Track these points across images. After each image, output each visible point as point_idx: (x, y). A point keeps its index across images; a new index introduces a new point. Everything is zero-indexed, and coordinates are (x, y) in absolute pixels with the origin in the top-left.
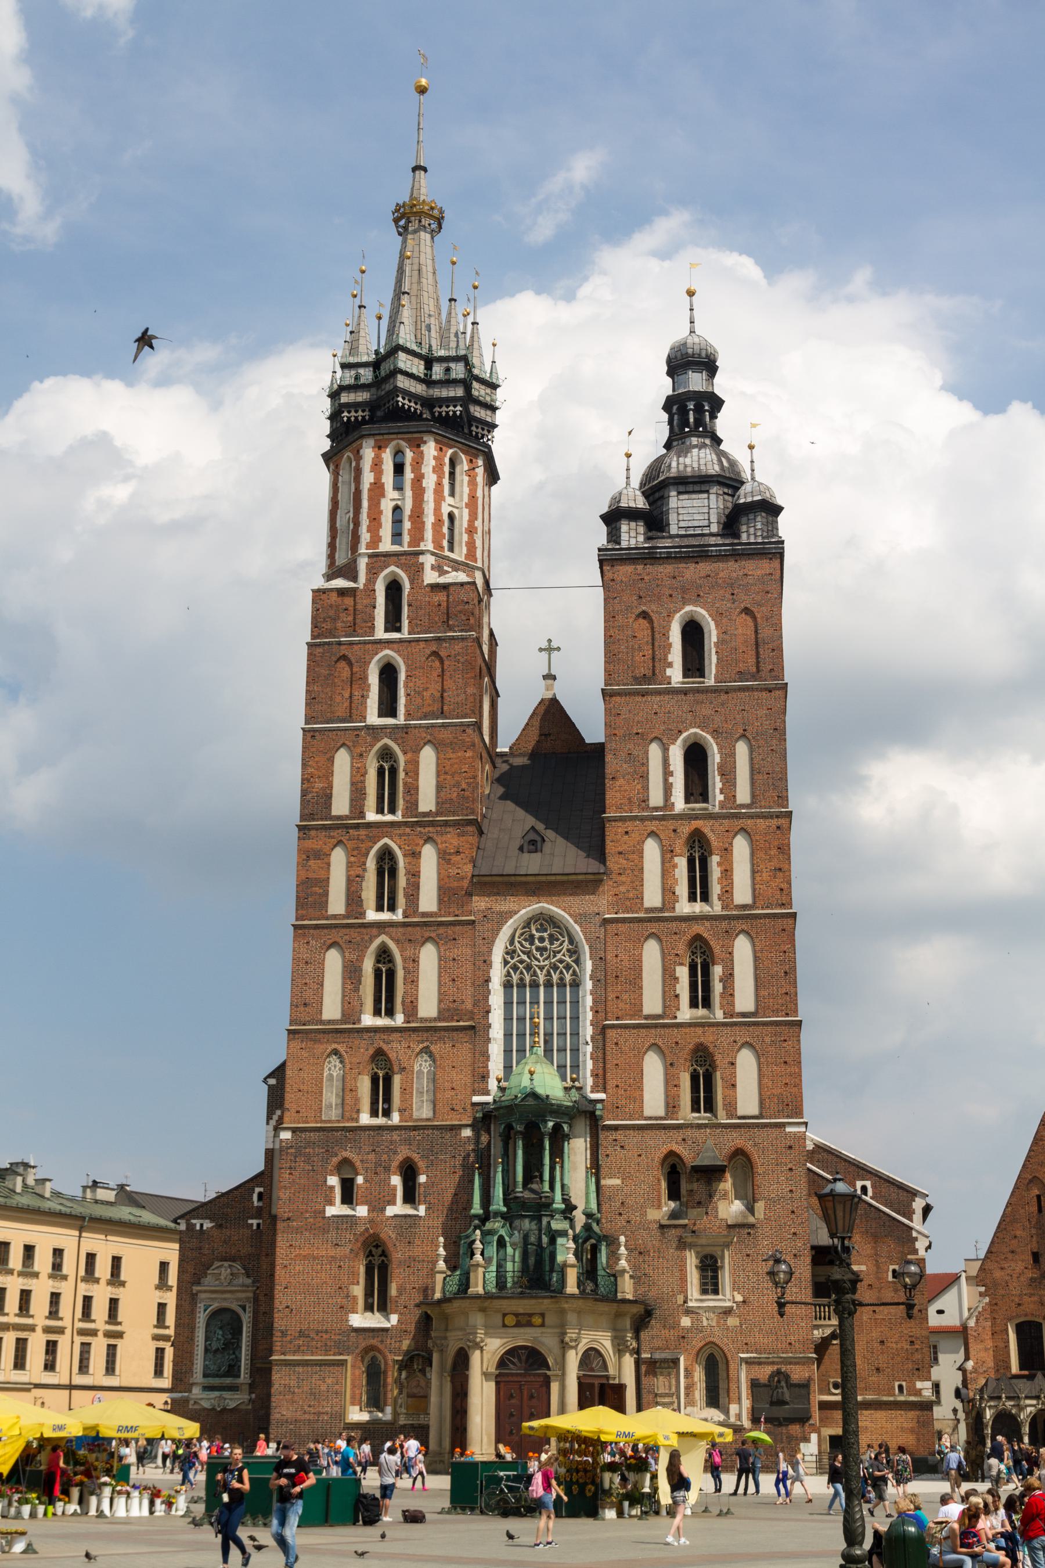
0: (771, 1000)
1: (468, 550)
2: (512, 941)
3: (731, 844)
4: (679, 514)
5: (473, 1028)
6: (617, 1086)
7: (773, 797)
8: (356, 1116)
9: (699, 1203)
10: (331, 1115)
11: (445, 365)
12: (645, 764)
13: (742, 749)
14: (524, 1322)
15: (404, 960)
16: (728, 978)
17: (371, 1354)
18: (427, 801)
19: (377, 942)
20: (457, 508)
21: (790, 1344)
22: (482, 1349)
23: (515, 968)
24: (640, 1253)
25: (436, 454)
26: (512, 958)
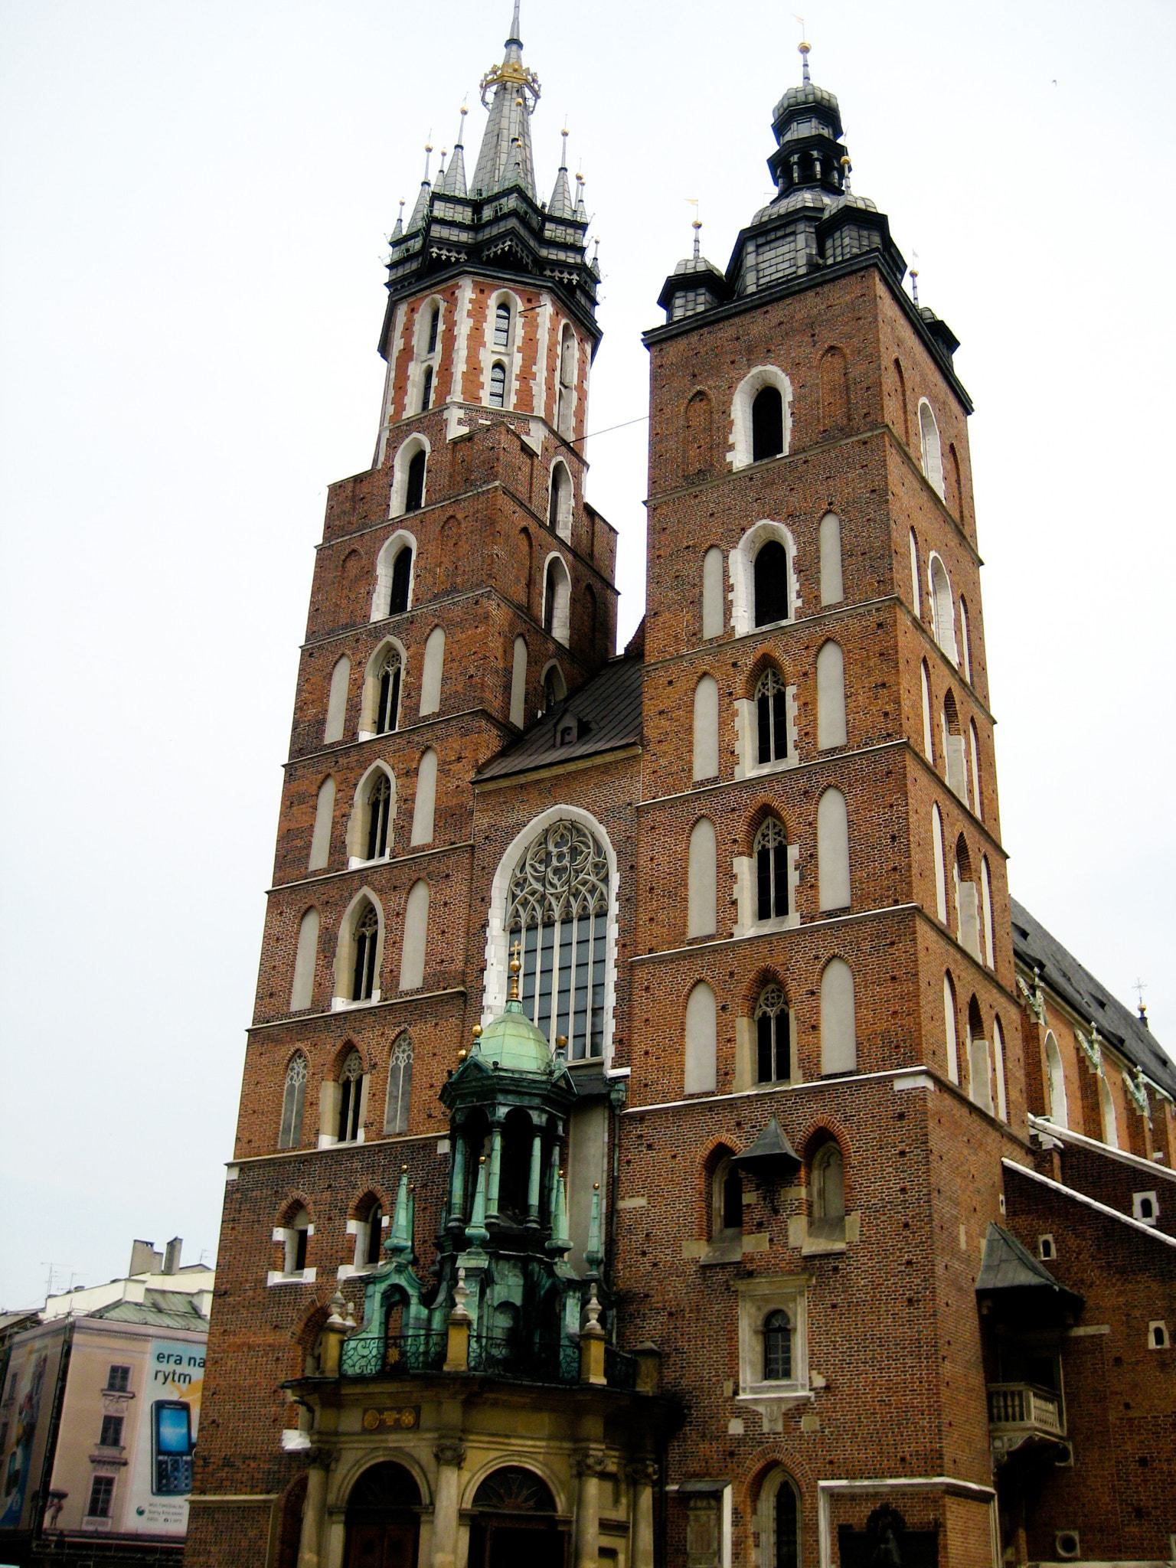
3: (814, 665)
4: (758, 271)
5: (462, 994)
6: (647, 1053)
7: (871, 584)
9: (760, 1225)
14: (390, 1422)
18: (429, 703)
20: (508, 355)
21: (903, 1459)
22: (327, 1469)
23: (525, 903)
24: (671, 1314)
25: (474, 296)
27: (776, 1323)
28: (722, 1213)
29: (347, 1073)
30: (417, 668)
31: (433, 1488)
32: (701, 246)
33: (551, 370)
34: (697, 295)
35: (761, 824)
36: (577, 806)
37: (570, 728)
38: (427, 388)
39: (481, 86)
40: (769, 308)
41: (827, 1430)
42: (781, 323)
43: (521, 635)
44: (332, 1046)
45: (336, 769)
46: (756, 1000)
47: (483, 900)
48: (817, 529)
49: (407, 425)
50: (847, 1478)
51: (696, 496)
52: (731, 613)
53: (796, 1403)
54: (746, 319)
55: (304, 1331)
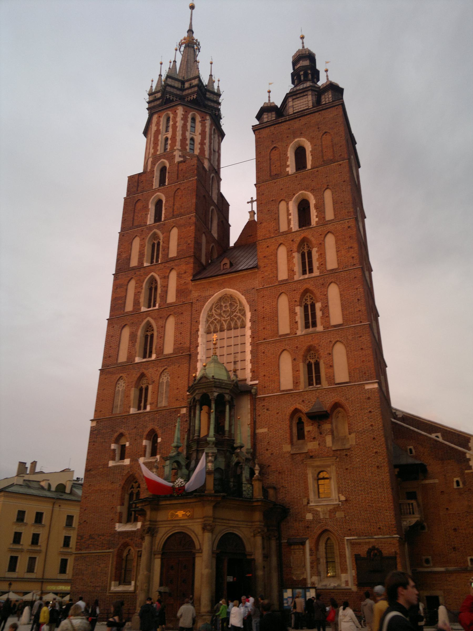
0: (351, 316)
1: (200, 151)
2: (211, 310)
3: (324, 240)
4: (293, 108)
5: (190, 355)
6: (264, 376)
8: (128, 410)
10: (118, 411)
11: (189, 82)
12: (278, 213)
13: (328, 195)
15: (158, 328)
16: (325, 308)
17: (128, 548)
18: (173, 253)
19: (145, 321)
21: (379, 528)
25: (183, 113)
26: (211, 319)
27: (321, 475)
28: (296, 434)
29: (142, 385)
30: (167, 241)
31: (201, 542)
32: (271, 99)
33: (210, 143)
34: (272, 114)
35: (305, 295)
36: (233, 289)
37: (226, 264)
38: (166, 144)
39: (179, 45)
40: (301, 118)
41: (347, 517)
42: (306, 124)
43: (204, 233)
44: (136, 375)
45: (135, 276)
46: (306, 356)
47: (196, 322)
48: (323, 194)
49: (159, 156)
50: (357, 536)
51: (275, 183)
52: (290, 223)
53: (333, 507)
54: (292, 122)
55: (124, 484)
